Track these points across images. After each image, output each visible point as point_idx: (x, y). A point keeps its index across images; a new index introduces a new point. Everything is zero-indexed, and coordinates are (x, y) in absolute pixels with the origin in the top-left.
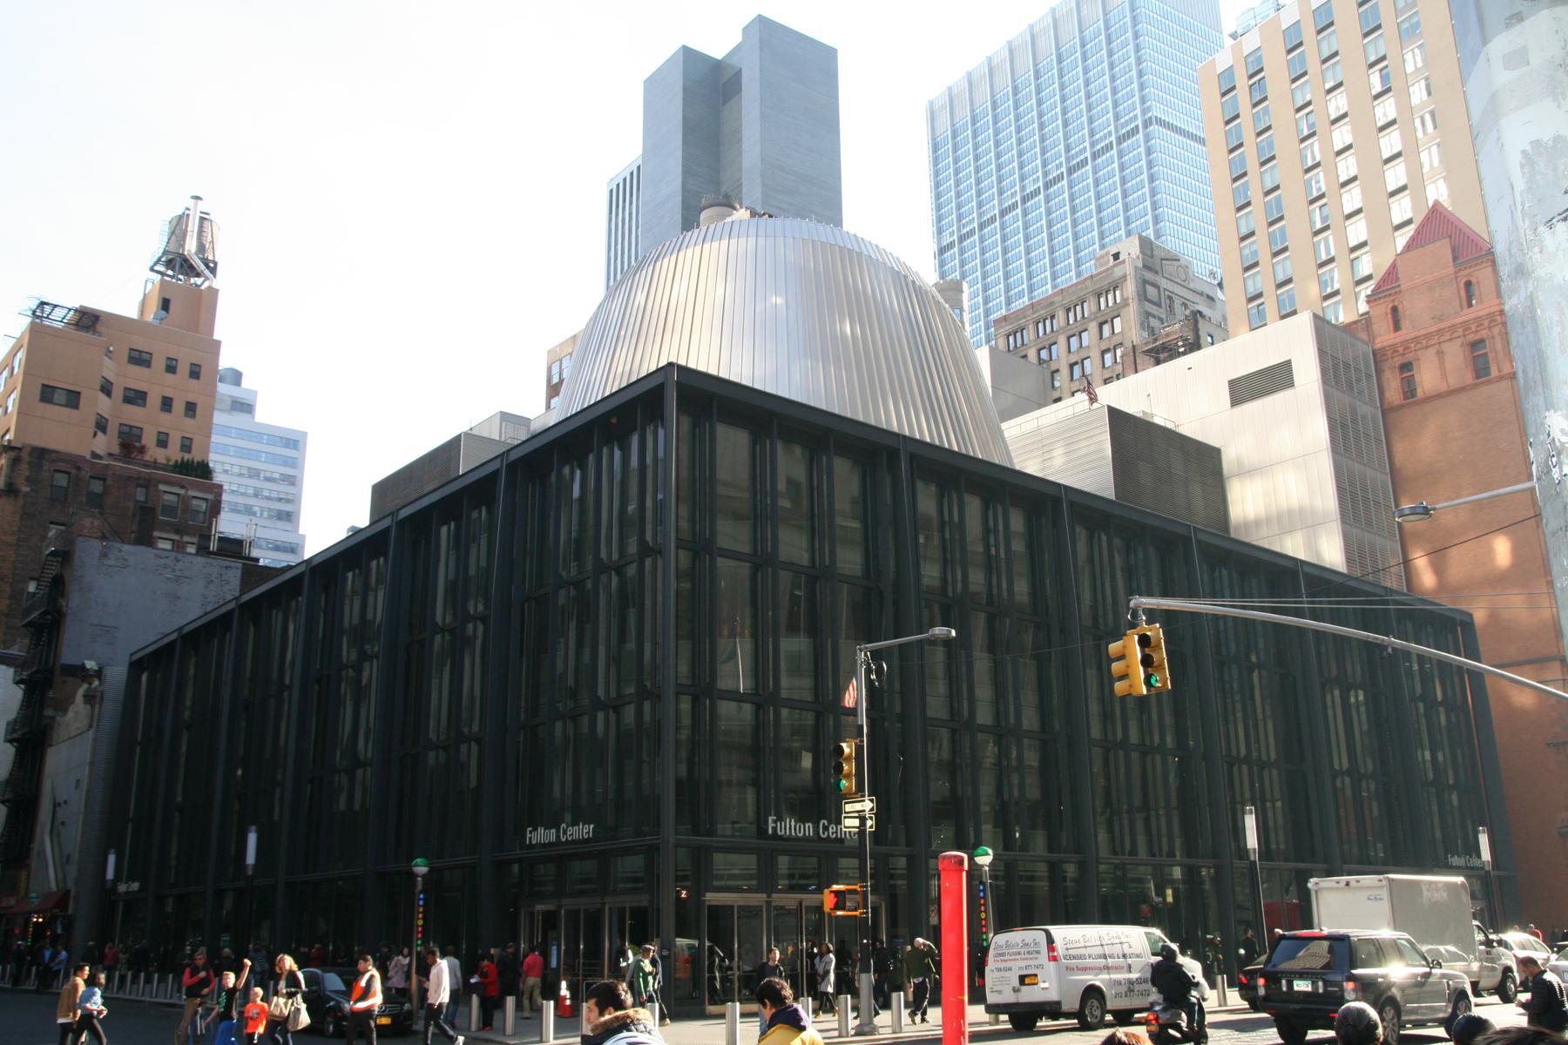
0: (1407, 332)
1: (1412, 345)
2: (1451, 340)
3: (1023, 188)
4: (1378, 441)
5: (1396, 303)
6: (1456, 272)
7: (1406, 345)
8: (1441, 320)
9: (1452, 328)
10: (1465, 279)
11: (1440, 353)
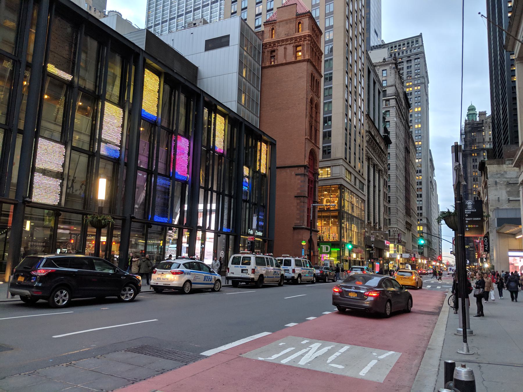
0: (275, 39)
1: (276, 44)
2: (290, 44)
3: (178, 12)
4: (258, 78)
5: (274, 27)
6: (296, 18)
7: (274, 43)
8: (288, 36)
9: (291, 39)
10: (299, 21)
11: (285, 48)
